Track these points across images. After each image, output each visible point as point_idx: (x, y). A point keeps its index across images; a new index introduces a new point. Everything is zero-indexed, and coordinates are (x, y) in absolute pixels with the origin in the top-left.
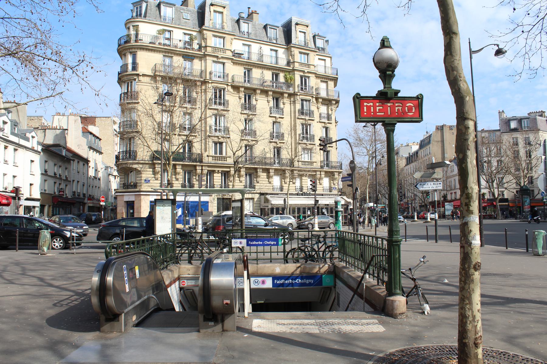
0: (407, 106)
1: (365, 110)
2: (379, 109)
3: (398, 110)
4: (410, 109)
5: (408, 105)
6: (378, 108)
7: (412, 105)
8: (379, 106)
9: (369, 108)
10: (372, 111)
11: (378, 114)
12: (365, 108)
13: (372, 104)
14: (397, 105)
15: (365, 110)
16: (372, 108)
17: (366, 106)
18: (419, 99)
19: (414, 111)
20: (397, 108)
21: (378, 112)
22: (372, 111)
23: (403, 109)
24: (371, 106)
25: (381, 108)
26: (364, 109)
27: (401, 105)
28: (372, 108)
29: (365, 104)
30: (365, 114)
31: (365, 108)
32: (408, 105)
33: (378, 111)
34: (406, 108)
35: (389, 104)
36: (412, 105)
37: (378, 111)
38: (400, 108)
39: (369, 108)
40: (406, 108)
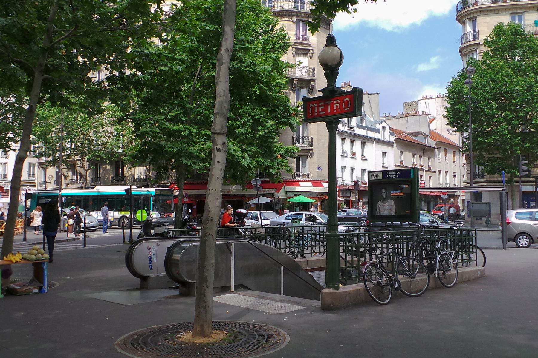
3: (337, 106)
7: (348, 99)
8: (322, 105)
10: (316, 111)
11: (320, 113)
12: (311, 109)
13: (315, 105)
14: (335, 102)
16: (316, 108)
20: (335, 105)
21: (320, 112)
22: (316, 111)
23: (341, 106)
27: (339, 101)
29: (311, 105)
31: (311, 109)
32: (344, 101)
33: (320, 110)
36: (348, 99)
38: (338, 105)
39: (313, 108)
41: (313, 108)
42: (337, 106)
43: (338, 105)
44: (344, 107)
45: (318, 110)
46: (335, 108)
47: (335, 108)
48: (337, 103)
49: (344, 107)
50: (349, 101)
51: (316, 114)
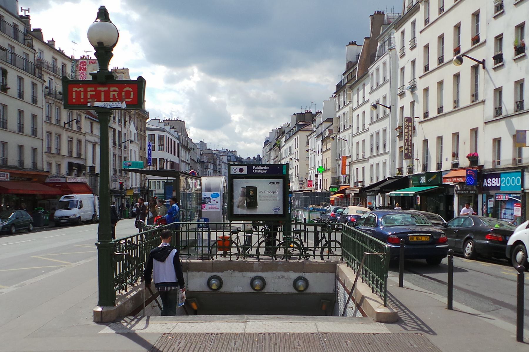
0: (124, 91)
1: (74, 97)
3: (114, 95)
5: (125, 89)
6: (89, 94)
7: (131, 90)
8: (91, 91)
9: (78, 93)
10: (82, 97)
12: (74, 93)
13: (82, 89)
14: (112, 89)
15: (74, 97)
16: (82, 94)
17: (76, 91)
18: (141, 81)
19: (132, 96)
20: (112, 93)
21: (89, 99)
22: (82, 97)
24: (80, 91)
25: (94, 93)
27: (117, 89)
28: (82, 94)
29: (75, 89)
31: (74, 93)
32: (125, 89)
33: (89, 97)
34: (123, 93)
35: (102, 89)
37: (89, 97)
38: (116, 93)
39: (78, 93)
40: (123, 93)
42: (114, 95)
43: (116, 93)
45: (86, 95)
46: (111, 97)
50: (132, 91)
51: (82, 100)
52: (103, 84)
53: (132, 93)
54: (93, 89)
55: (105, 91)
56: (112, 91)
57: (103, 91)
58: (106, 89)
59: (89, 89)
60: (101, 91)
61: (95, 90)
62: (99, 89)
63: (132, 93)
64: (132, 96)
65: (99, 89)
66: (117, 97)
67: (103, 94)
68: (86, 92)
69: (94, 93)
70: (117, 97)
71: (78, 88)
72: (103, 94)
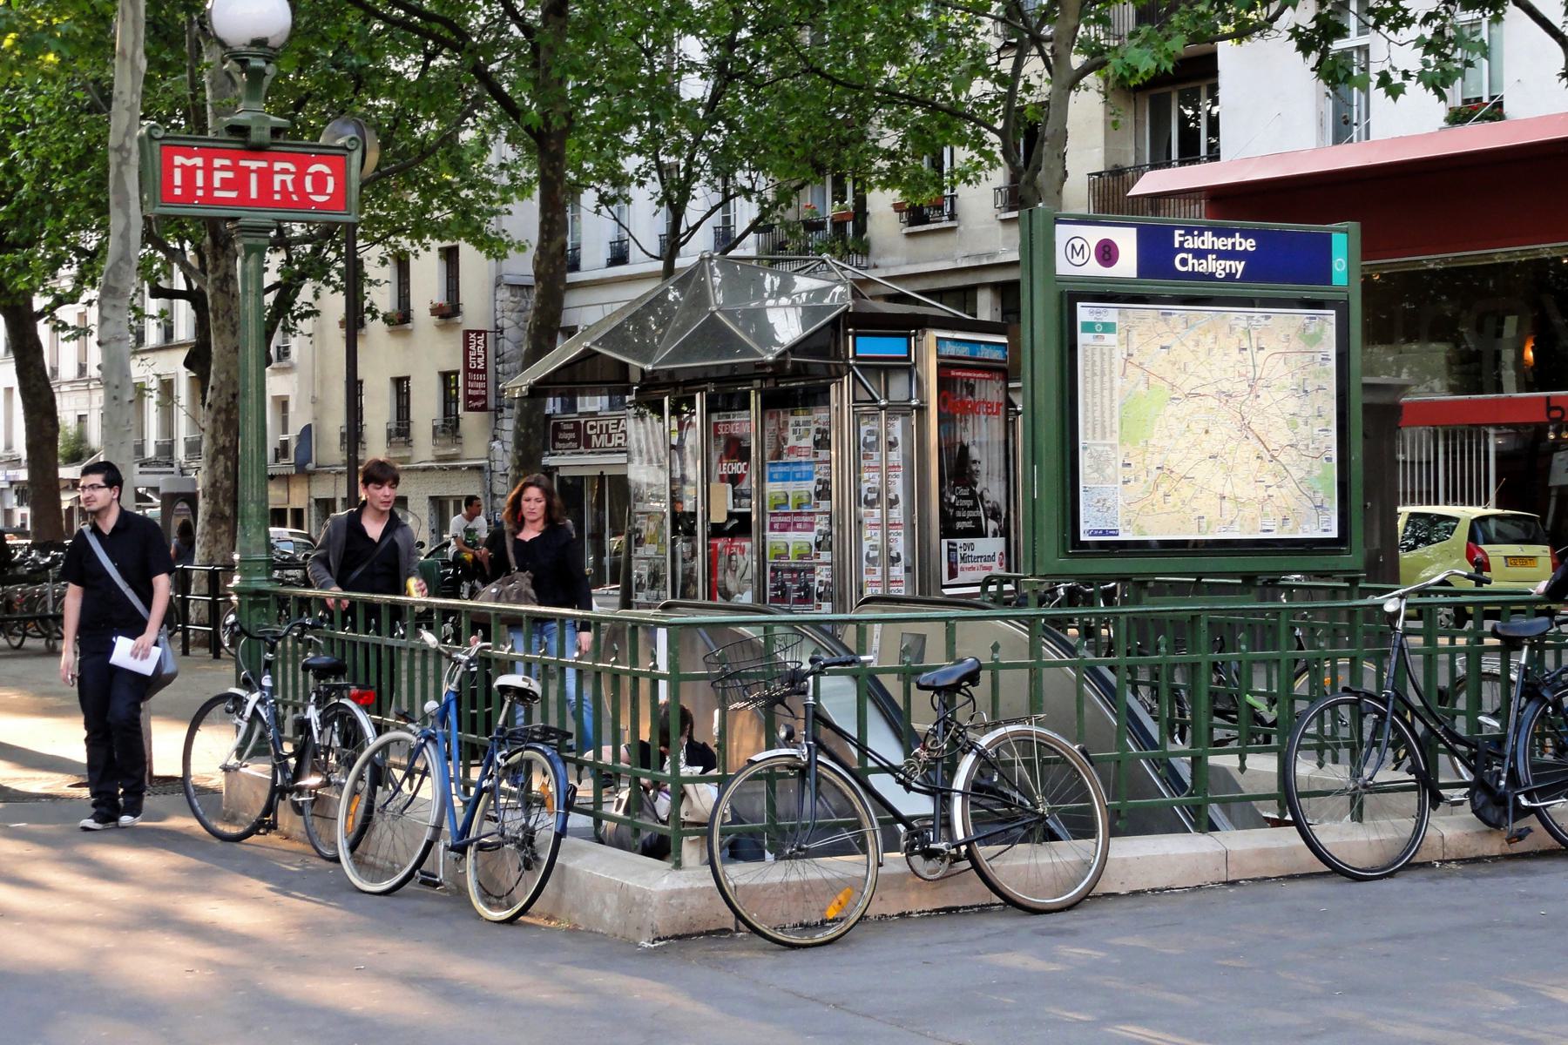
1: (178, 180)
2: (223, 180)
3: (283, 183)
4: (319, 180)
5: (313, 169)
6: (218, 177)
7: (326, 169)
8: (223, 168)
9: (189, 173)
10: (200, 182)
11: (217, 194)
13: (199, 161)
14: (278, 166)
15: (178, 180)
16: (200, 175)
17: (182, 166)
19: (330, 188)
20: (277, 179)
21: (217, 189)
22: (200, 182)
23: (299, 182)
24: (195, 167)
25: (230, 175)
26: (172, 176)
28: (200, 175)
29: (178, 160)
30: (178, 192)
32: (313, 169)
33: (217, 184)
34: (308, 181)
35: (254, 165)
36: (326, 169)
37: (217, 184)
40: (308, 181)
41: (189, 173)
42: (283, 183)
43: (289, 178)
44: (309, 188)
45: (208, 178)
46: (277, 187)
47: (277, 187)
48: (285, 171)
49: (309, 188)
51: (200, 193)
52: (257, 150)
53: (331, 182)
54: (227, 162)
55: (259, 171)
56: (278, 172)
57: (253, 171)
58: (264, 164)
59: (217, 163)
60: (248, 170)
61: (234, 168)
62: (243, 163)
63: (331, 182)
64: (330, 188)
65: (243, 163)
66: (291, 188)
67: (253, 178)
68: (209, 171)
69: (230, 175)
70: (291, 188)
71: (189, 157)
72: (253, 178)
